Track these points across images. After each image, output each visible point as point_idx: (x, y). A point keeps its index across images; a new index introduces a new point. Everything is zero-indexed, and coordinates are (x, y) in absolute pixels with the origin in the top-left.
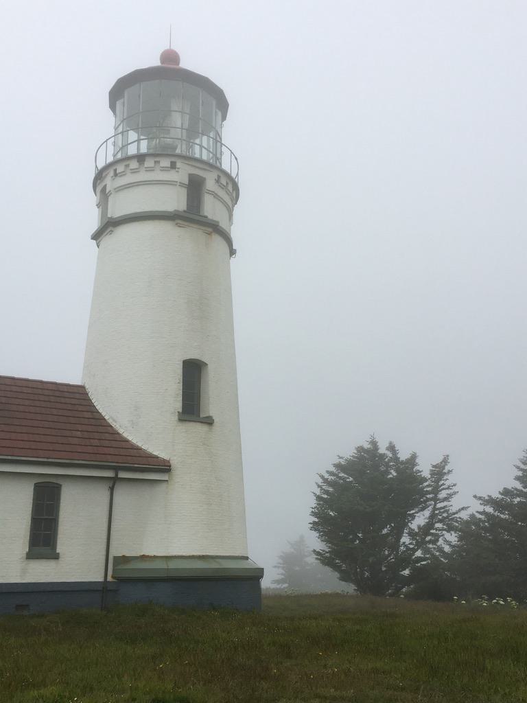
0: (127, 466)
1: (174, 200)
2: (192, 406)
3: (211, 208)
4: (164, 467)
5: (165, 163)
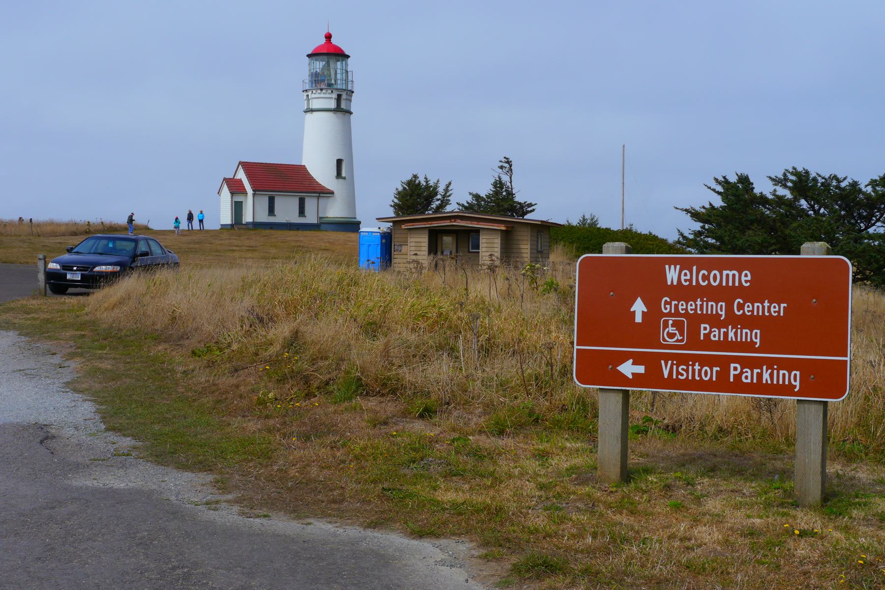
0: (323, 193)
1: (332, 104)
2: (339, 175)
3: (343, 106)
4: (332, 193)
5: (330, 91)
